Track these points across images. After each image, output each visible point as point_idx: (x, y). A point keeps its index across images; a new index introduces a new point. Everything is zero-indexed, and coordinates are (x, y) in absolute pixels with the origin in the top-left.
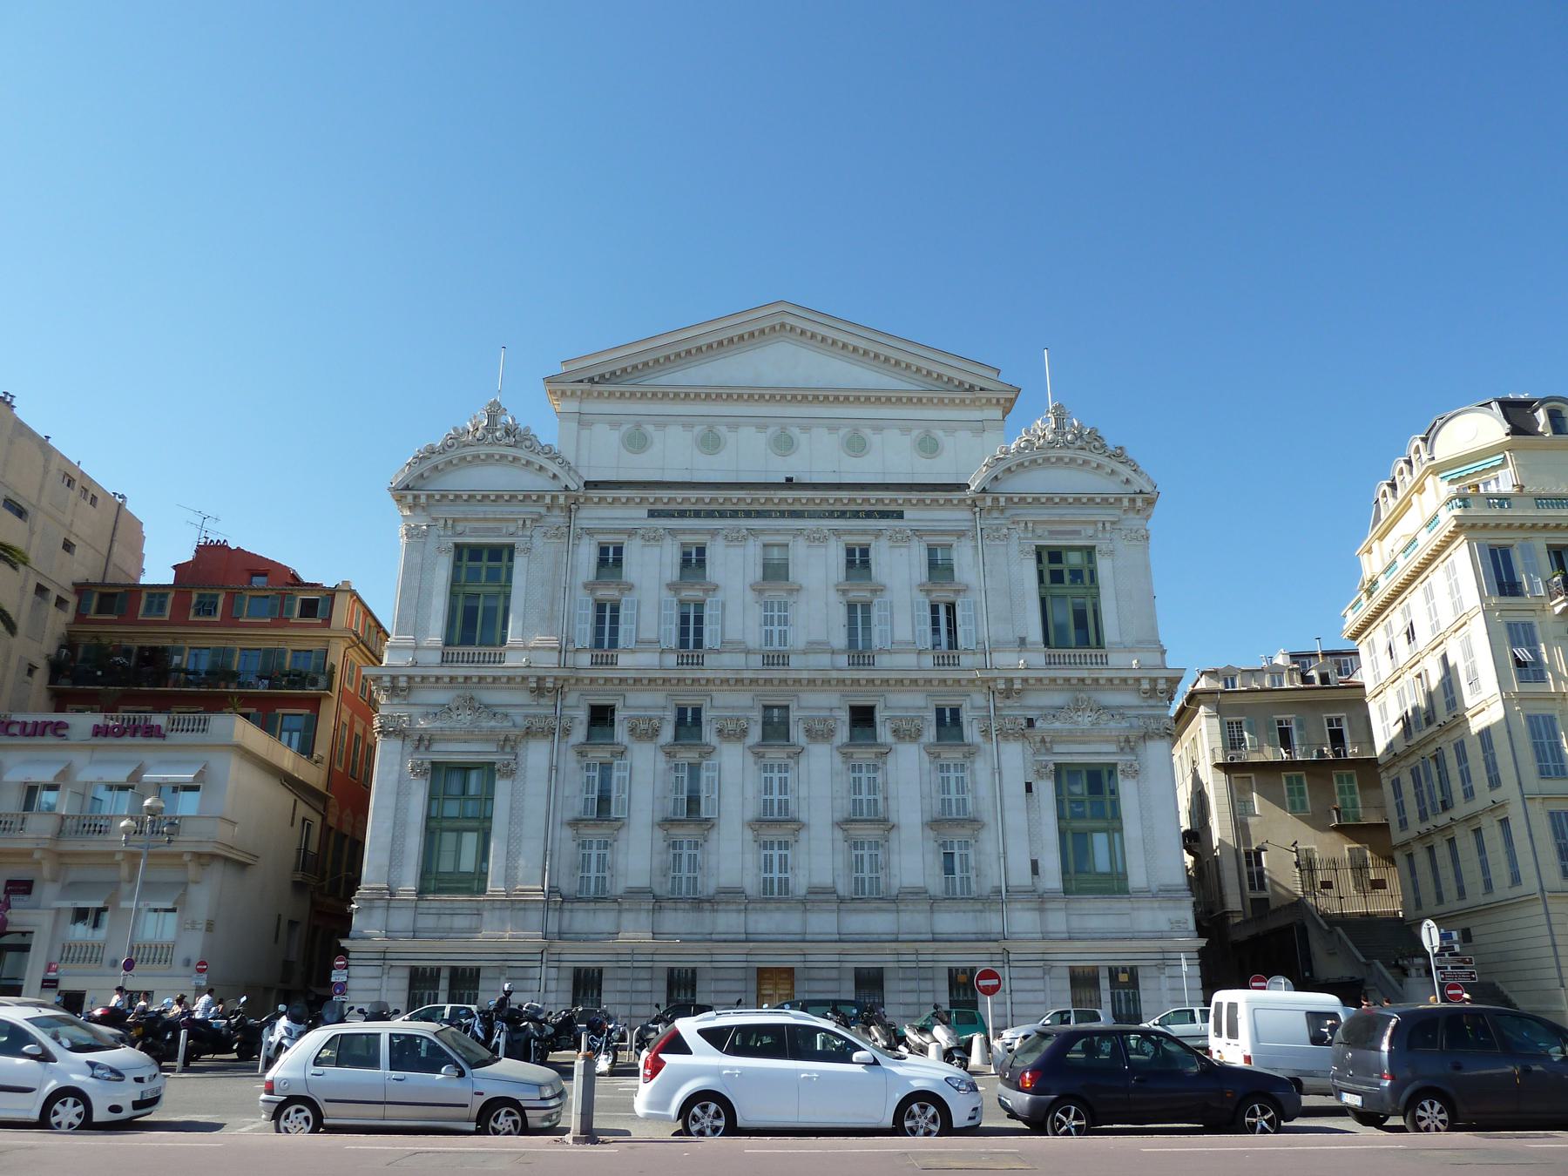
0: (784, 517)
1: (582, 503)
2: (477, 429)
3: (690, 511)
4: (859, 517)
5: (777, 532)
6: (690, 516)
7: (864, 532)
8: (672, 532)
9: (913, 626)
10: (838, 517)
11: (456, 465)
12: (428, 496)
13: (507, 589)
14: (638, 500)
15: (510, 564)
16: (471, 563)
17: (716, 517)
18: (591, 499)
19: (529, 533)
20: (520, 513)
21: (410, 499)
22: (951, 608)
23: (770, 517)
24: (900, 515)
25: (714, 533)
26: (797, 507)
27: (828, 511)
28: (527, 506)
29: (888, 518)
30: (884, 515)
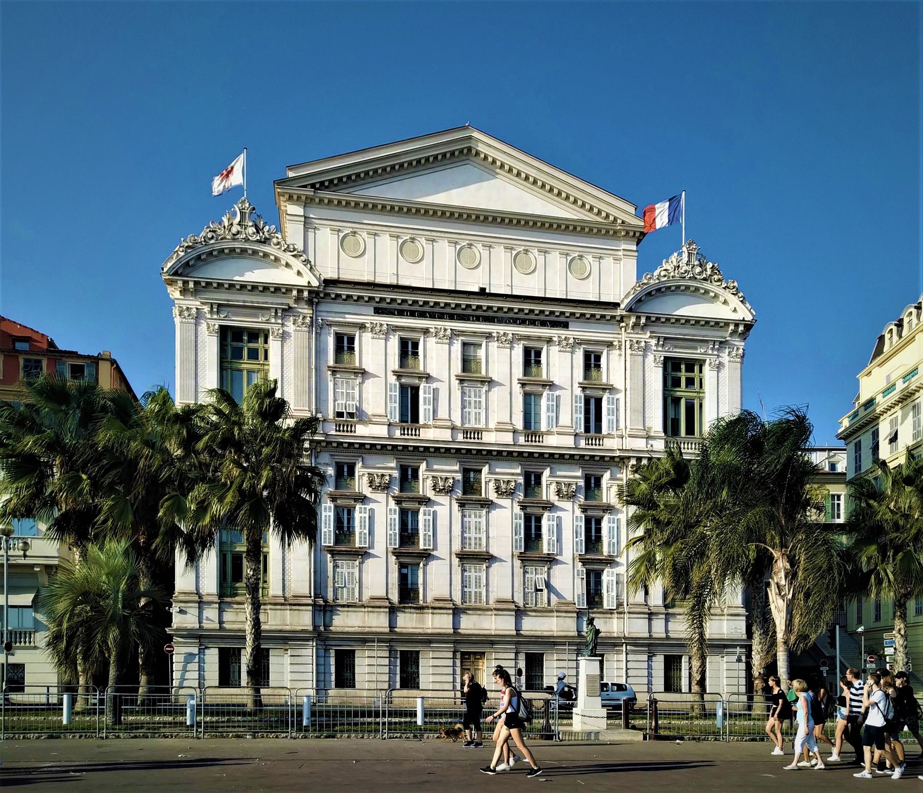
0: (479, 321)
1: (322, 298)
2: (232, 224)
3: (407, 311)
4: (535, 325)
5: (474, 334)
6: (407, 315)
7: (539, 339)
8: (396, 329)
9: (572, 415)
10: (520, 324)
11: (216, 256)
12: (196, 283)
13: (266, 367)
14: (366, 299)
15: (266, 346)
16: (234, 343)
17: (427, 317)
18: (329, 294)
19: (280, 321)
20: (272, 303)
21: (180, 284)
22: (599, 402)
23: (469, 320)
24: (565, 325)
25: (426, 331)
26: (490, 314)
27: (511, 318)
28: (278, 297)
29: (557, 327)
30: (555, 324)
